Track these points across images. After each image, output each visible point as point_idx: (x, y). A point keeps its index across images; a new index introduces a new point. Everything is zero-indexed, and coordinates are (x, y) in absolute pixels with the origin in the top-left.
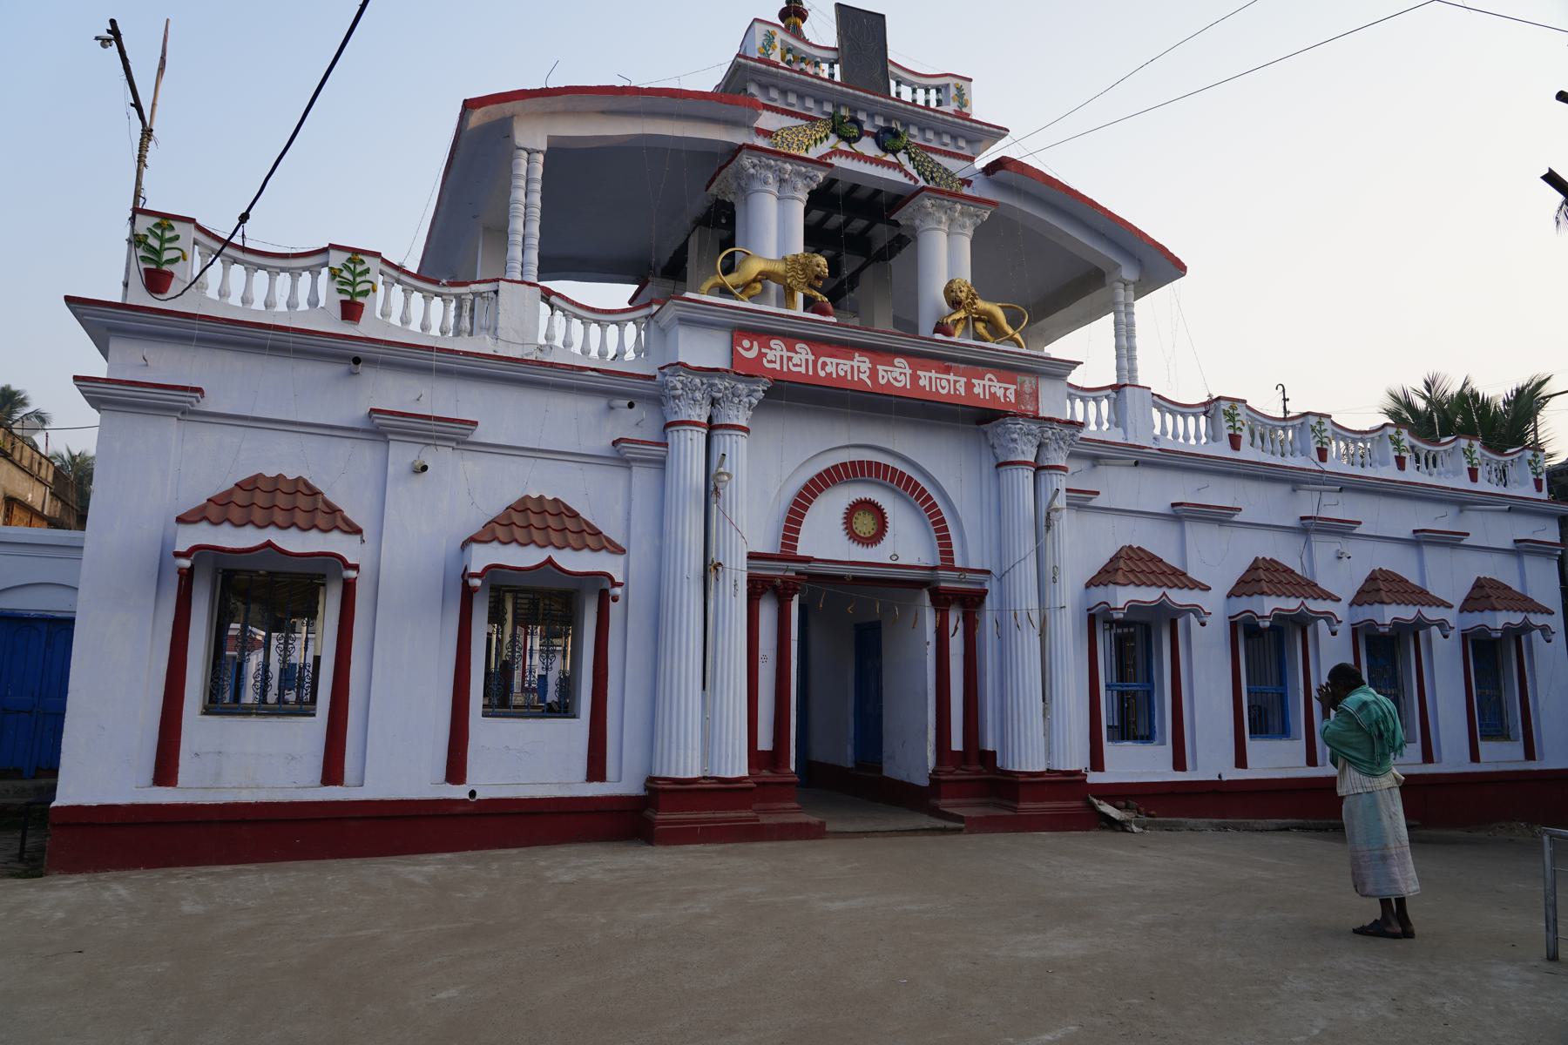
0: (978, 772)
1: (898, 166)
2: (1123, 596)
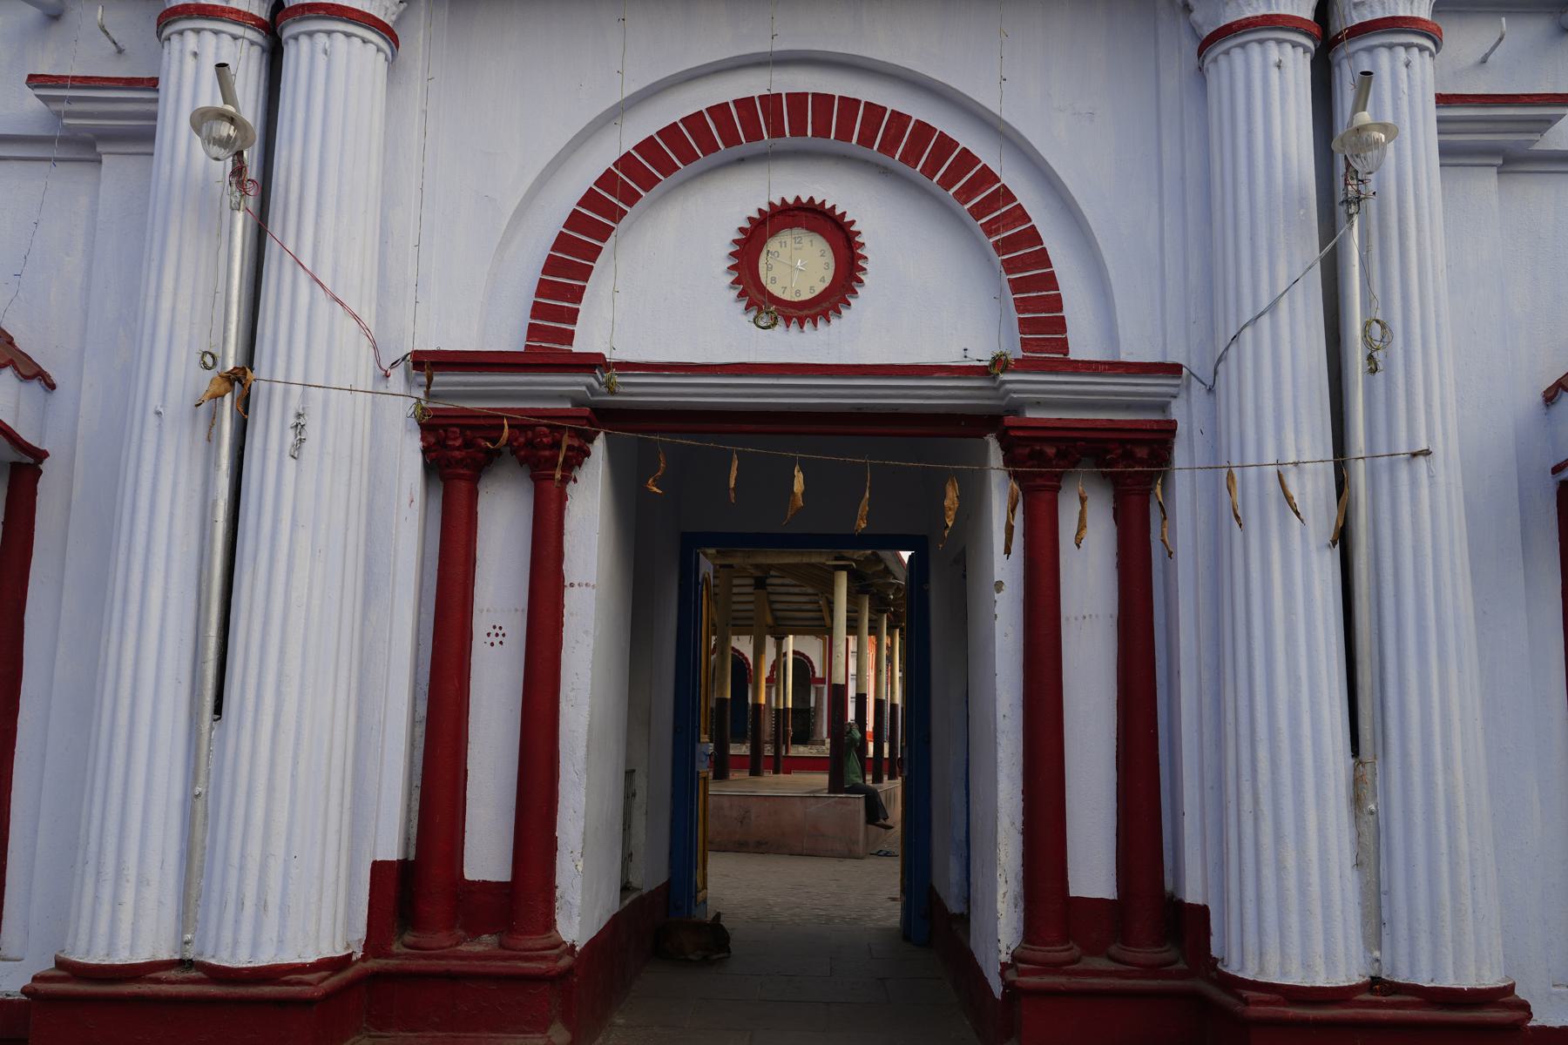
0: (1154, 970)
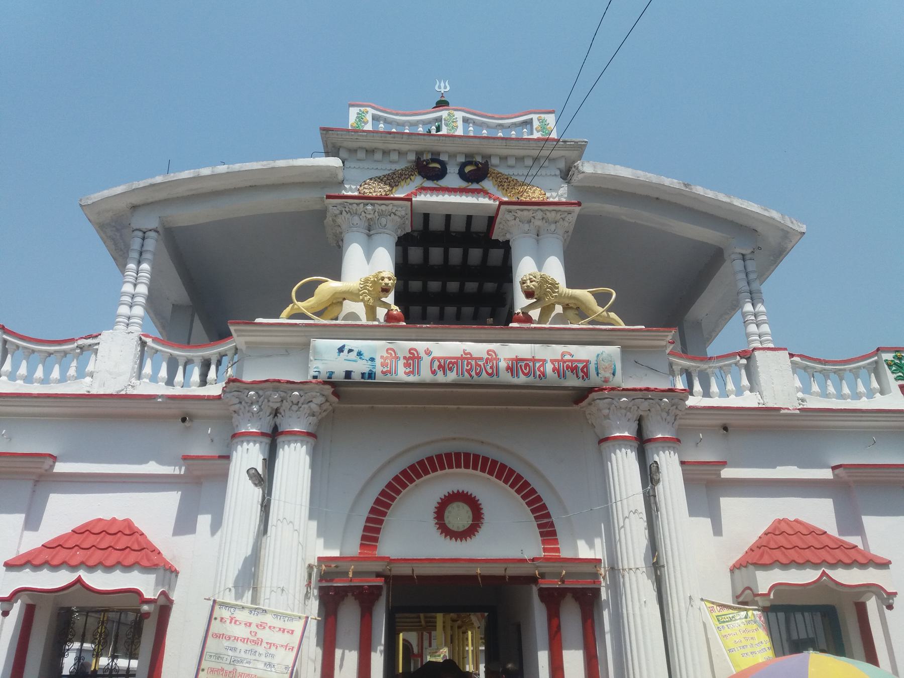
1: (485, 193)
2: (766, 580)
